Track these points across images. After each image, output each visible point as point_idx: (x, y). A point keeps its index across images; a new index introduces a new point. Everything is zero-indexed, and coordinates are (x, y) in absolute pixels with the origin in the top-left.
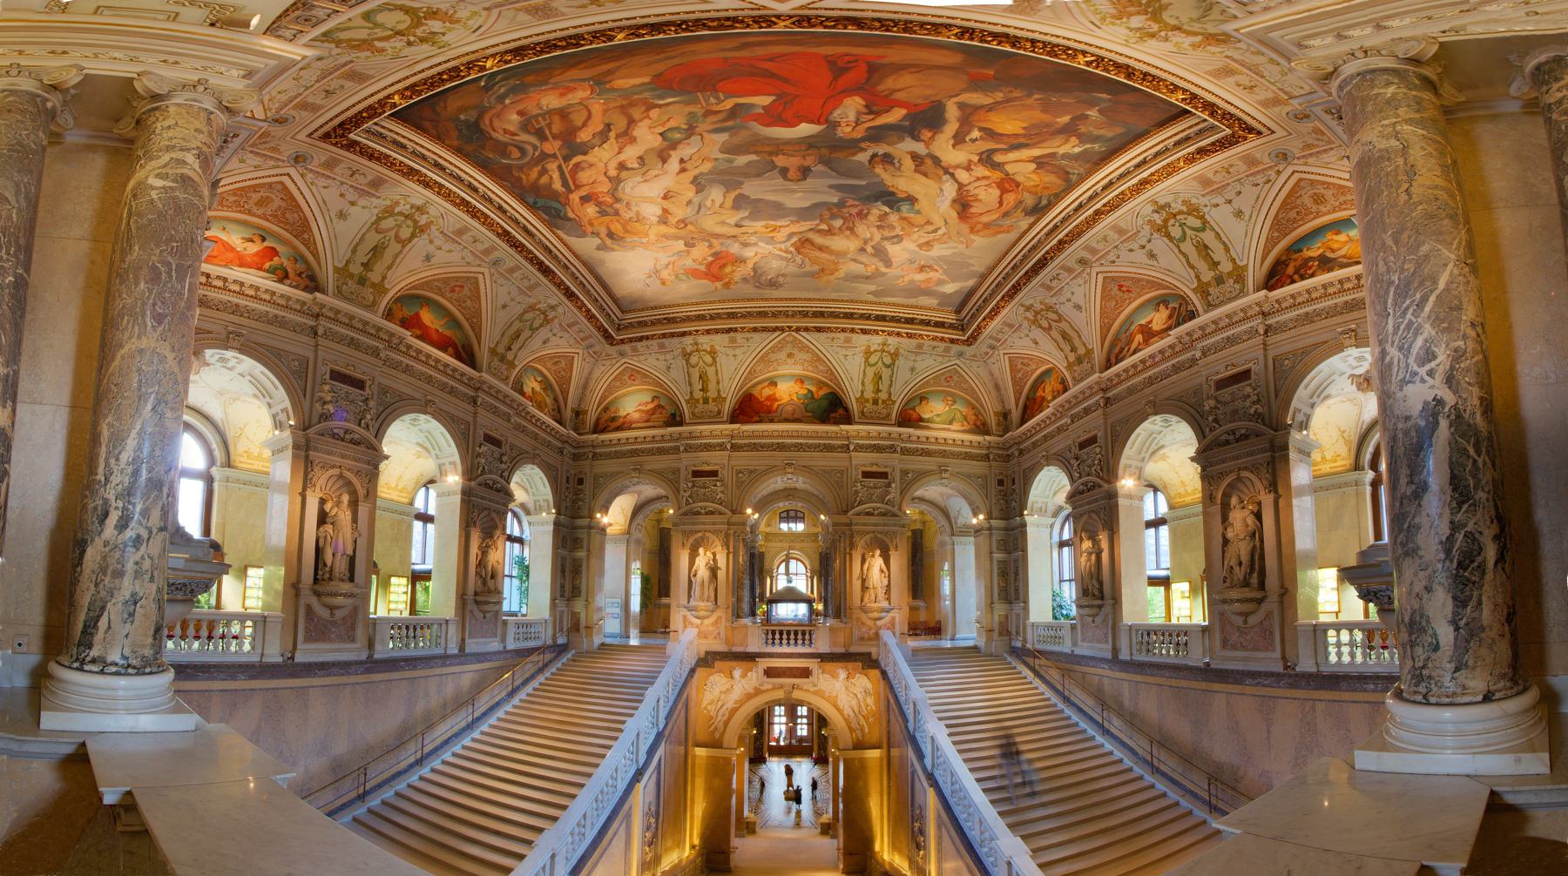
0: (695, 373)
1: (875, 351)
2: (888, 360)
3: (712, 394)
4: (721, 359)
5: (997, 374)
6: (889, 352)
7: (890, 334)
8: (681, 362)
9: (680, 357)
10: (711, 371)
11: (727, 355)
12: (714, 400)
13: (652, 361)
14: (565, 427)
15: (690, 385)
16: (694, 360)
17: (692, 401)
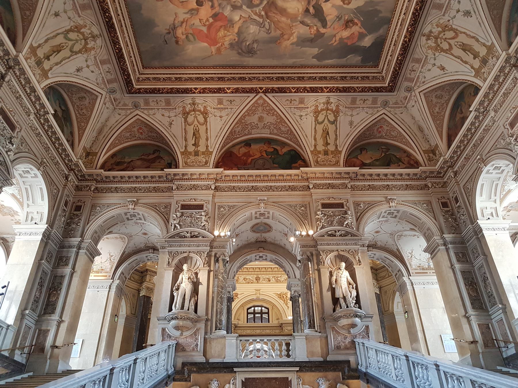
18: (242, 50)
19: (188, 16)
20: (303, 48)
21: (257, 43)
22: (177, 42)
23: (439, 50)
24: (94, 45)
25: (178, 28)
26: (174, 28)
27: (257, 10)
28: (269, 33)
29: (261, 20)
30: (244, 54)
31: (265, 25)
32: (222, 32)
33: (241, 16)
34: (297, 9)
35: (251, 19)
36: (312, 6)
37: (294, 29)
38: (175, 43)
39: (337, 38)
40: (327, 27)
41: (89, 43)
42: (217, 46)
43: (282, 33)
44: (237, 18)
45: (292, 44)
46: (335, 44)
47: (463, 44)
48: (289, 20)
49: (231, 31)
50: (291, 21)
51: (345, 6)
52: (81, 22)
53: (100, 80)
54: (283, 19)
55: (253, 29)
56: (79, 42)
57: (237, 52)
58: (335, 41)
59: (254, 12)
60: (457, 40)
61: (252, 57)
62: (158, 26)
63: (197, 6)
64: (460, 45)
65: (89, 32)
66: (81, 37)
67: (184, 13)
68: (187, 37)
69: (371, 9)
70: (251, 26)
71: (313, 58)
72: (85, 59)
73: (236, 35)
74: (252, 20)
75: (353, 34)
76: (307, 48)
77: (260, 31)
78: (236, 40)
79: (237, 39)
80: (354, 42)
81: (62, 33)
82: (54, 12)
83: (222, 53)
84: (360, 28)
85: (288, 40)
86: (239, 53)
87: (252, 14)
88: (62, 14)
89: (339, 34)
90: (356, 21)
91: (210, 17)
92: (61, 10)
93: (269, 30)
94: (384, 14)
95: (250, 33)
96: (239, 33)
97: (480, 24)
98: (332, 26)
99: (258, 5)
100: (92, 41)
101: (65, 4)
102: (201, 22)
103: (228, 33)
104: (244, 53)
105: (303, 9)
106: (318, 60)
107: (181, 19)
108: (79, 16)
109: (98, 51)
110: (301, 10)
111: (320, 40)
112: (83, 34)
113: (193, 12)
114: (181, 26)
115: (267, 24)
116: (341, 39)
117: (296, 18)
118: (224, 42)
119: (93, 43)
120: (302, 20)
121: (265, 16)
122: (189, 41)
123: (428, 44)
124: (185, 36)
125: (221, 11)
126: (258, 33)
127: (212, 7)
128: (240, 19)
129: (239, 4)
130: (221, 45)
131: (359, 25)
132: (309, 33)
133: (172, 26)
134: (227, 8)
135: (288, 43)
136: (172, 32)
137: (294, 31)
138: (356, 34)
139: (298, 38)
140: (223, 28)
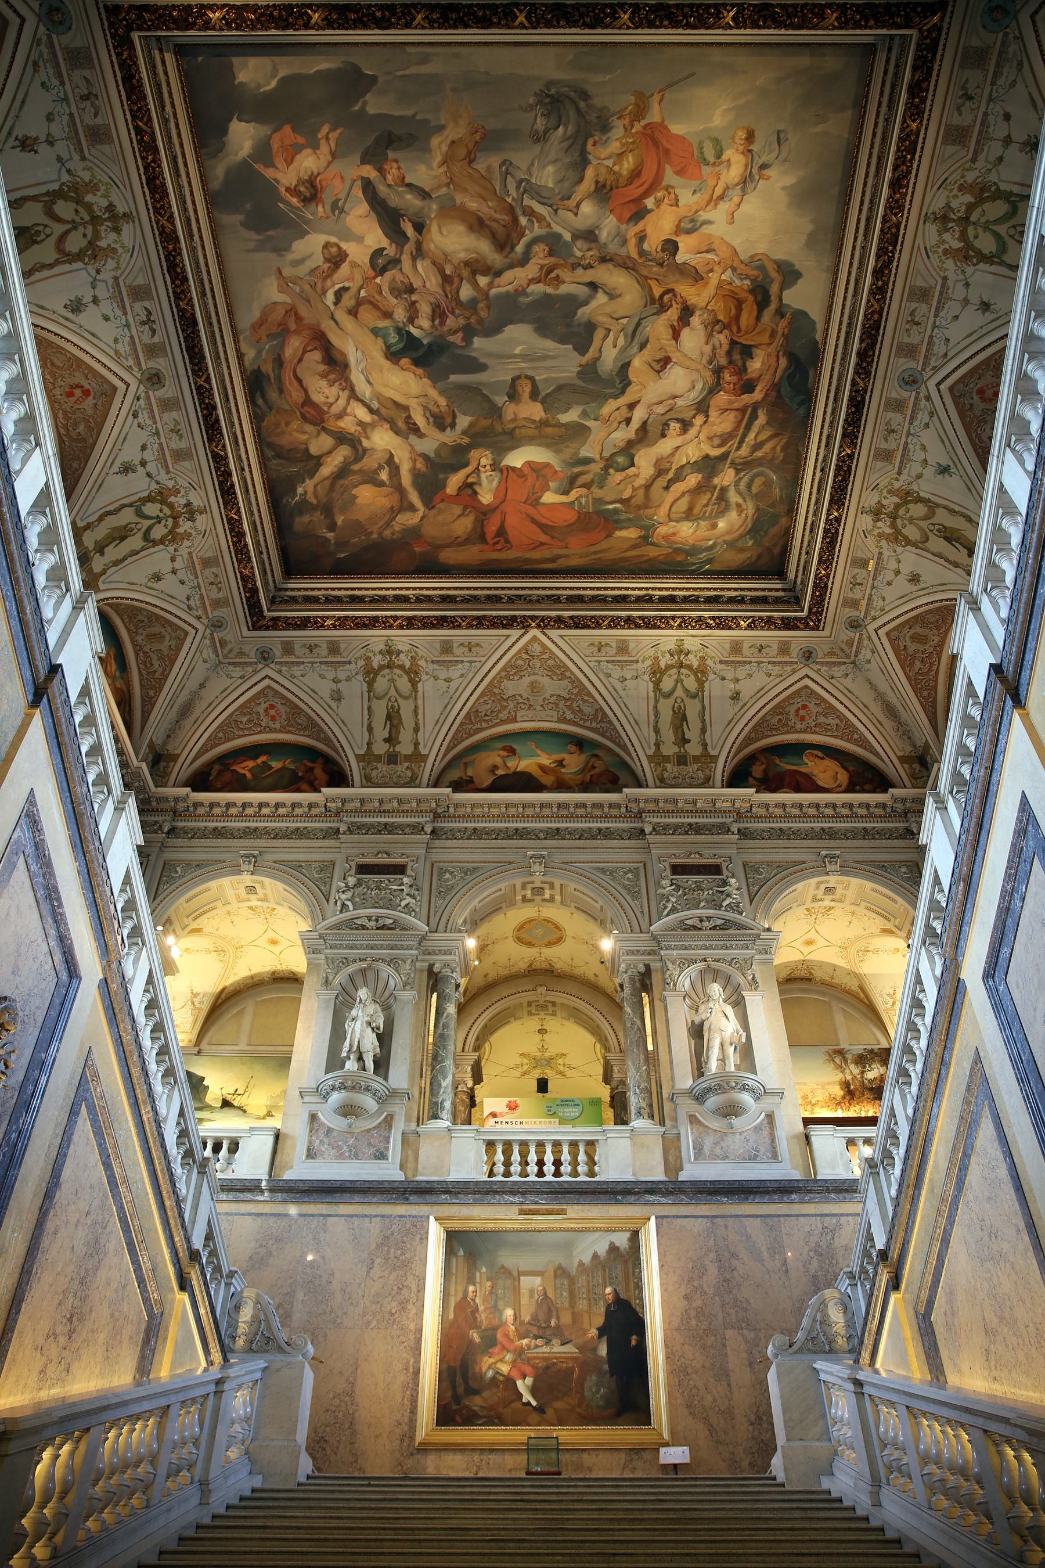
0: (380, 710)
1: (669, 667)
2: (691, 684)
3: (405, 748)
4: (426, 685)
5: (884, 687)
6: (689, 667)
7: (684, 624)
8: (359, 685)
9: (360, 677)
10: (406, 710)
11: (436, 678)
12: (408, 758)
13: (312, 680)
14: (137, 755)
15: (370, 729)
16: (381, 684)
17: (367, 758)
18: (578, 111)
19: (704, 216)
20: (408, 113)
21: (537, 132)
22: (750, 137)
23: (69, 191)
24: (955, 197)
25: (737, 180)
26: (746, 182)
27: (538, 230)
28: (504, 163)
29: (527, 201)
30: (572, 94)
31: (518, 188)
32: (626, 165)
33: (576, 214)
34: (445, 232)
35: (551, 206)
36: (407, 239)
37: (443, 178)
38: (756, 134)
39: (324, 149)
40: (359, 183)
41: (963, 208)
42: (643, 123)
43: (471, 162)
44: (587, 208)
45: (441, 128)
46: (325, 129)
47: (35, 242)
48: (458, 202)
49: (603, 170)
50: (453, 200)
51: (333, 239)
52: (950, 264)
53: (1008, 73)
54: (473, 205)
55: (547, 177)
56: (983, 220)
57: (590, 102)
58: (327, 139)
59: (544, 223)
60: (53, 240)
61: (550, 84)
62: (784, 188)
63: (677, 239)
64: (38, 233)
65: (947, 236)
66: (971, 231)
67: (710, 222)
68: (719, 156)
69: (270, 233)
70: (550, 185)
71: (374, 79)
72: (1000, 168)
73: (590, 157)
74: (550, 202)
75: (289, 162)
76: (396, 113)
77: (529, 171)
78: (590, 142)
79: (590, 147)
80: (277, 137)
81: (1002, 263)
82: (987, 314)
83: (633, 99)
84: (278, 182)
85: (453, 142)
86: (585, 96)
87: (548, 219)
88: (975, 299)
89: (323, 163)
90: (294, 201)
91: (651, 211)
92: (971, 308)
93: (507, 173)
94: (231, 220)
95: (554, 162)
96: (583, 162)
97: (42, 308)
98: (348, 183)
99: (535, 241)
100: (952, 210)
101: (956, 317)
102: (676, 196)
103: (609, 163)
104: (572, 100)
105: (429, 231)
106: (357, 69)
107: (724, 206)
108: (945, 279)
109: (956, 175)
110: (434, 228)
111: (370, 141)
112: (963, 236)
113: (689, 226)
114: (727, 188)
115: (513, 192)
116: (315, 146)
117: (442, 208)
118: (624, 137)
119: (954, 204)
120: (427, 202)
121: (519, 211)
122: (717, 140)
123: (105, 196)
124: (724, 157)
125: (624, 227)
126: (532, 164)
127: (642, 238)
128: (578, 206)
129: (579, 243)
130: (632, 126)
131: (283, 190)
132: (402, 165)
133: (750, 187)
134: (609, 234)
135: (453, 132)
136: (755, 171)
137: (442, 170)
138: (280, 162)
139: (427, 150)
140: (622, 182)
